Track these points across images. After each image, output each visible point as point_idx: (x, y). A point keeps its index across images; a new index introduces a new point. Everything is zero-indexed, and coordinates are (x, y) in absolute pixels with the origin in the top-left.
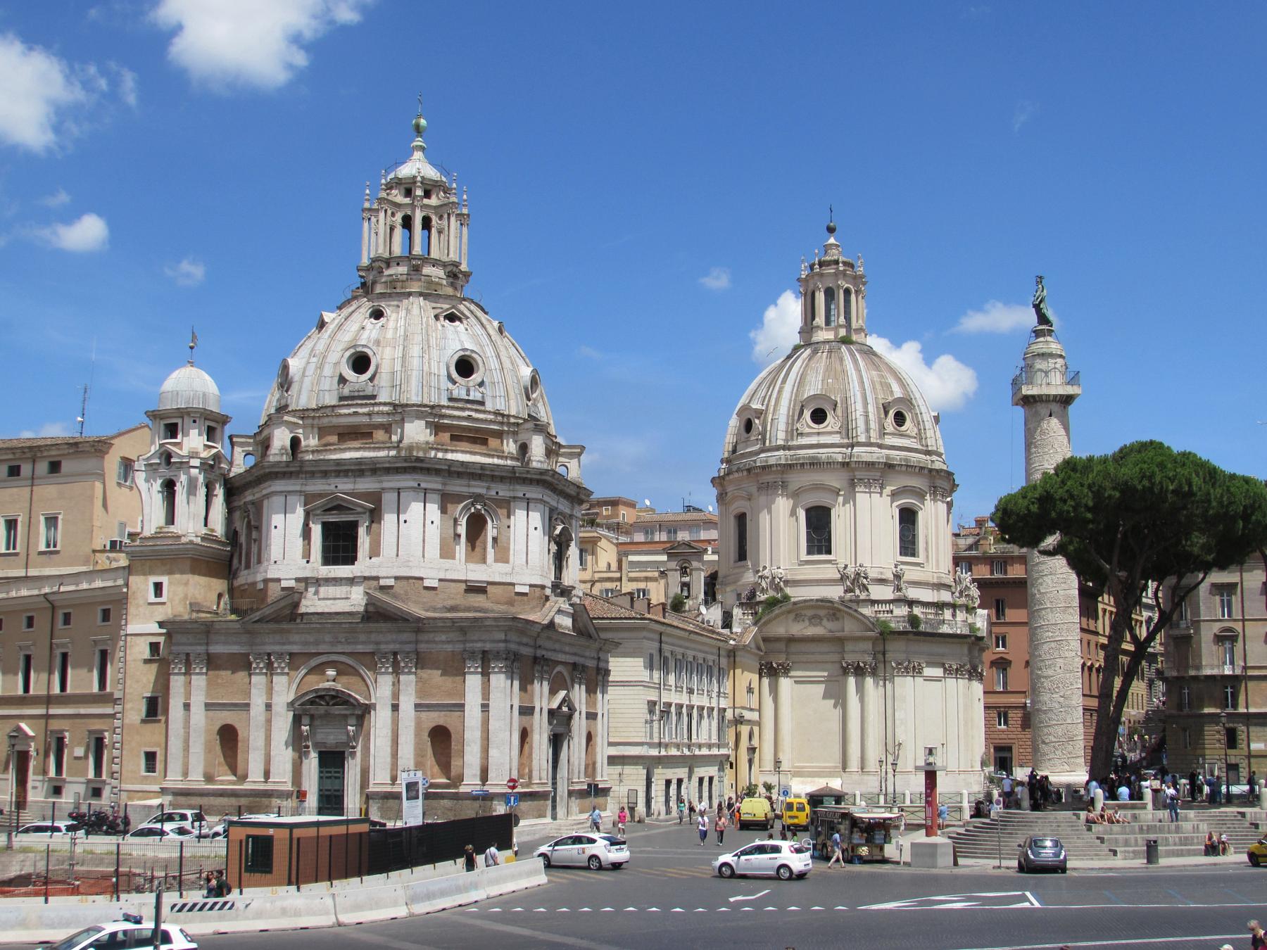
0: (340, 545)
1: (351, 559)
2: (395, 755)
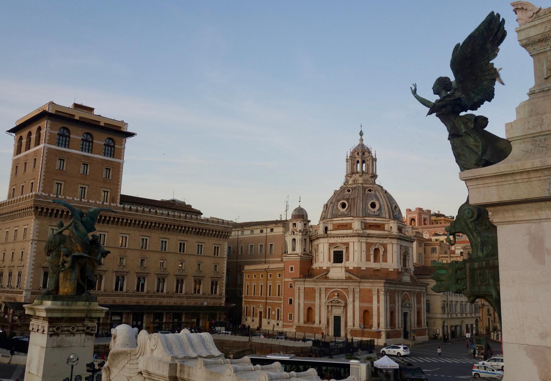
0: (338, 257)
1: (341, 262)
2: (354, 318)
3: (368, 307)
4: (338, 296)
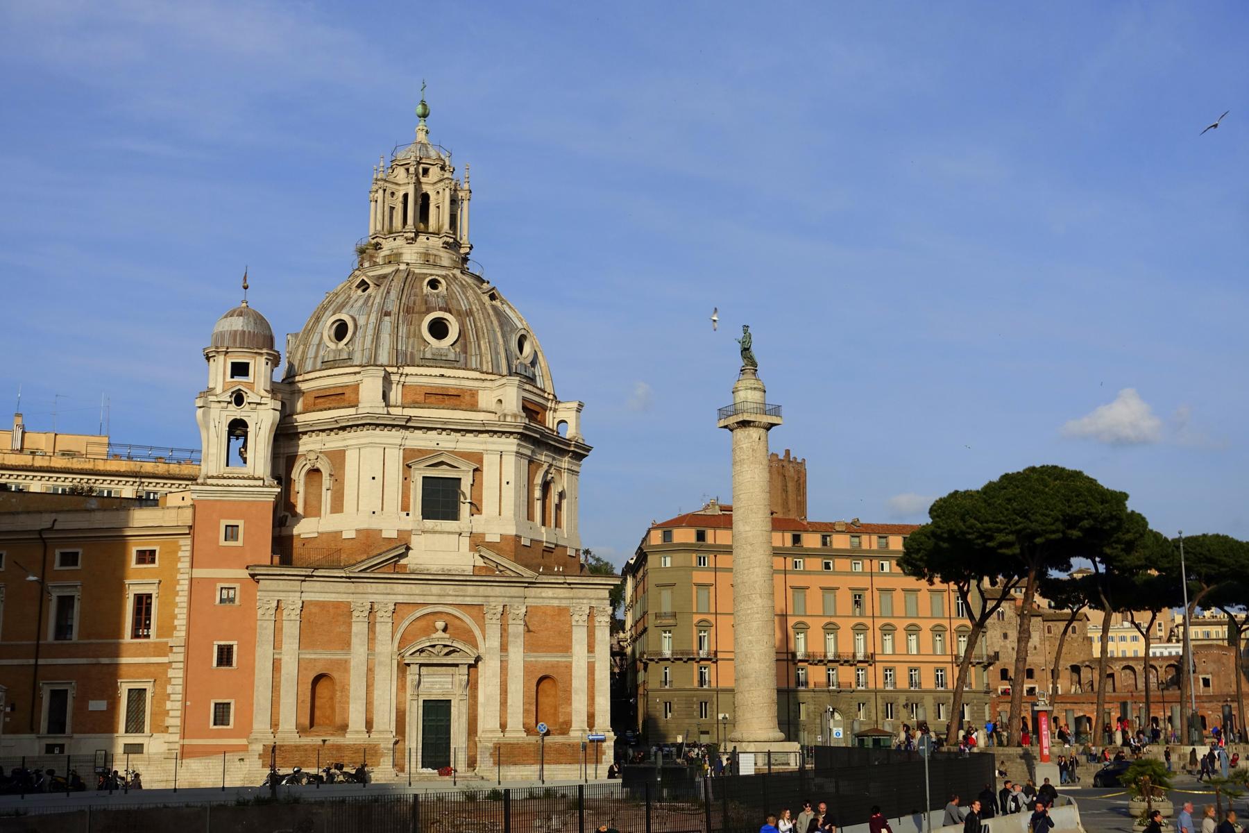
1: (454, 515)
2: (504, 703)
3: (555, 666)
4: (445, 630)
